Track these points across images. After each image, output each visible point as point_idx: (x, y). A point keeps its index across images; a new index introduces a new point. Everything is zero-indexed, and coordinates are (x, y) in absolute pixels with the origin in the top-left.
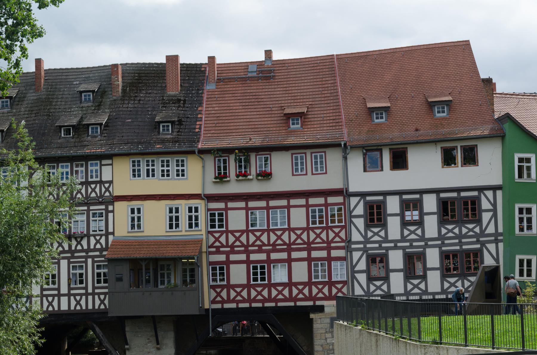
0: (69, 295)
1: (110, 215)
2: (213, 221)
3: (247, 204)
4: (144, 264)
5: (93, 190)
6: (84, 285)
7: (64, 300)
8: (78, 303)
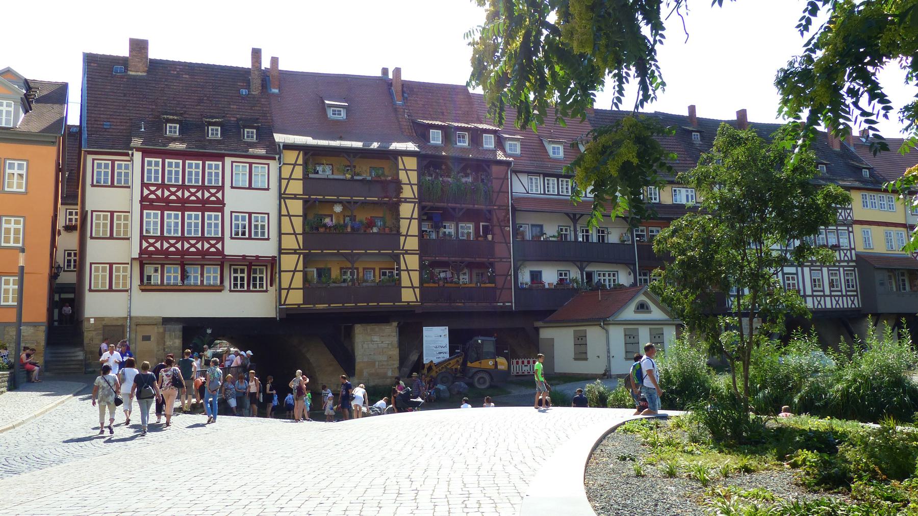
0: (831, 296)
1: (851, 234)
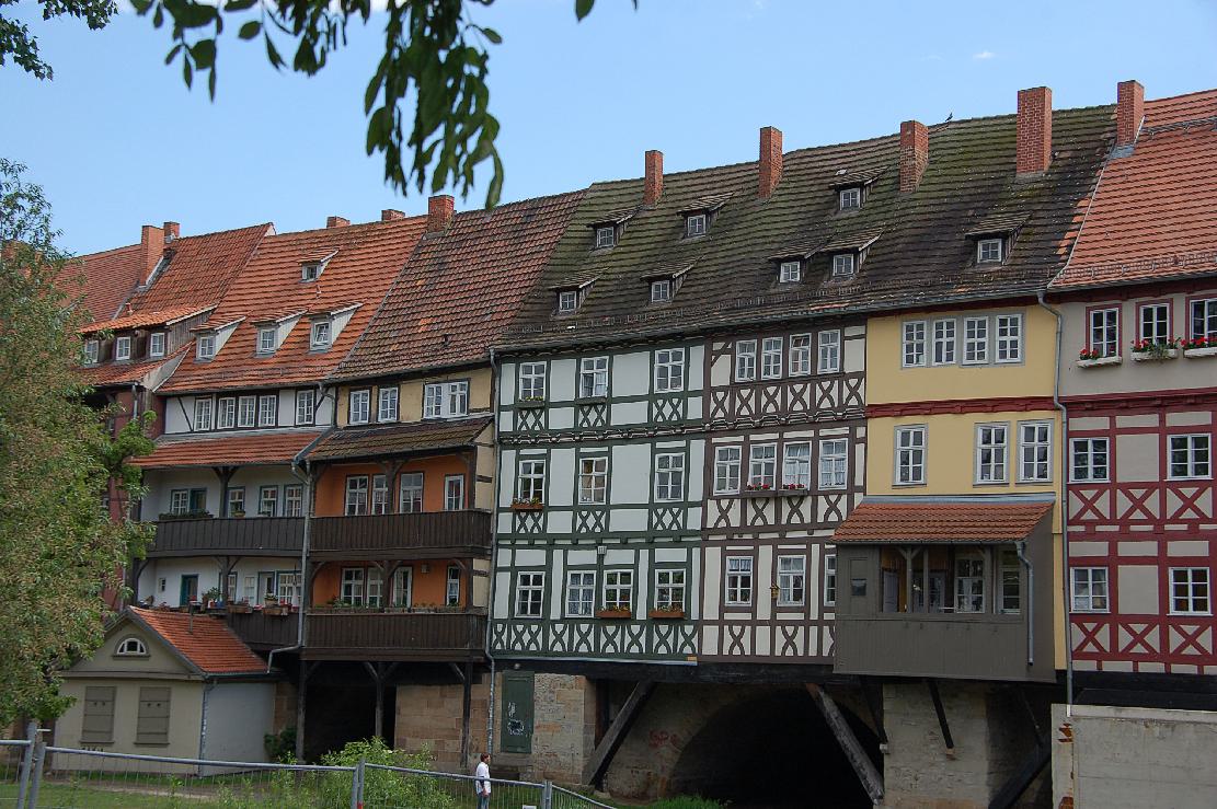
0: (773, 623)
1: (860, 448)
2: (1080, 459)
3: (1162, 420)
4: (909, 556)
5: (826, 393)
6: (801, 603)
7: (763, 633)
8: (790, 641)
